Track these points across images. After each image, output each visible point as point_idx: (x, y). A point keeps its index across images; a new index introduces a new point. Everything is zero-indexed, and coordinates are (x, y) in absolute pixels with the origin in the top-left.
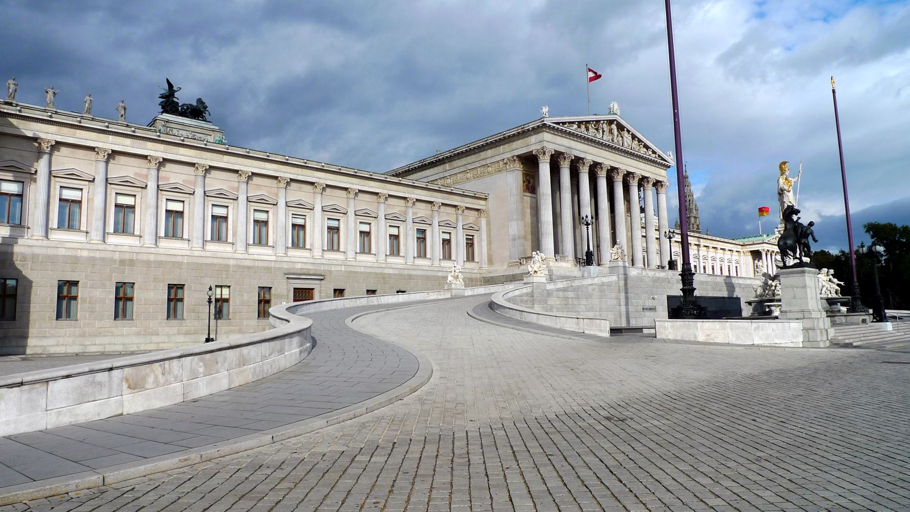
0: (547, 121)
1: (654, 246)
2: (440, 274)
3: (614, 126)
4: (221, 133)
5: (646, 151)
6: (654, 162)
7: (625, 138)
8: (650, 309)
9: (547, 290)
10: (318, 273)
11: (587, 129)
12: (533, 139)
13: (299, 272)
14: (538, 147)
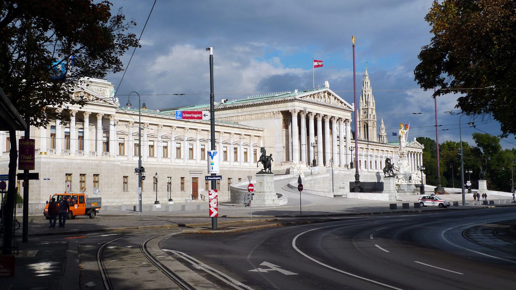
0: (297, 97)
1: (343, 156)
2: (244, 170)
3: (326, 94)
4: (113, 87)
5: (341, 104)
6: (345, 110)
7: (331, 100)
8: (342, 188)
9: (305, 181)
10: (200, 170)
11: (314, 98)
12: (290, 104)
13: (193, 170)
14: (292, 109)
